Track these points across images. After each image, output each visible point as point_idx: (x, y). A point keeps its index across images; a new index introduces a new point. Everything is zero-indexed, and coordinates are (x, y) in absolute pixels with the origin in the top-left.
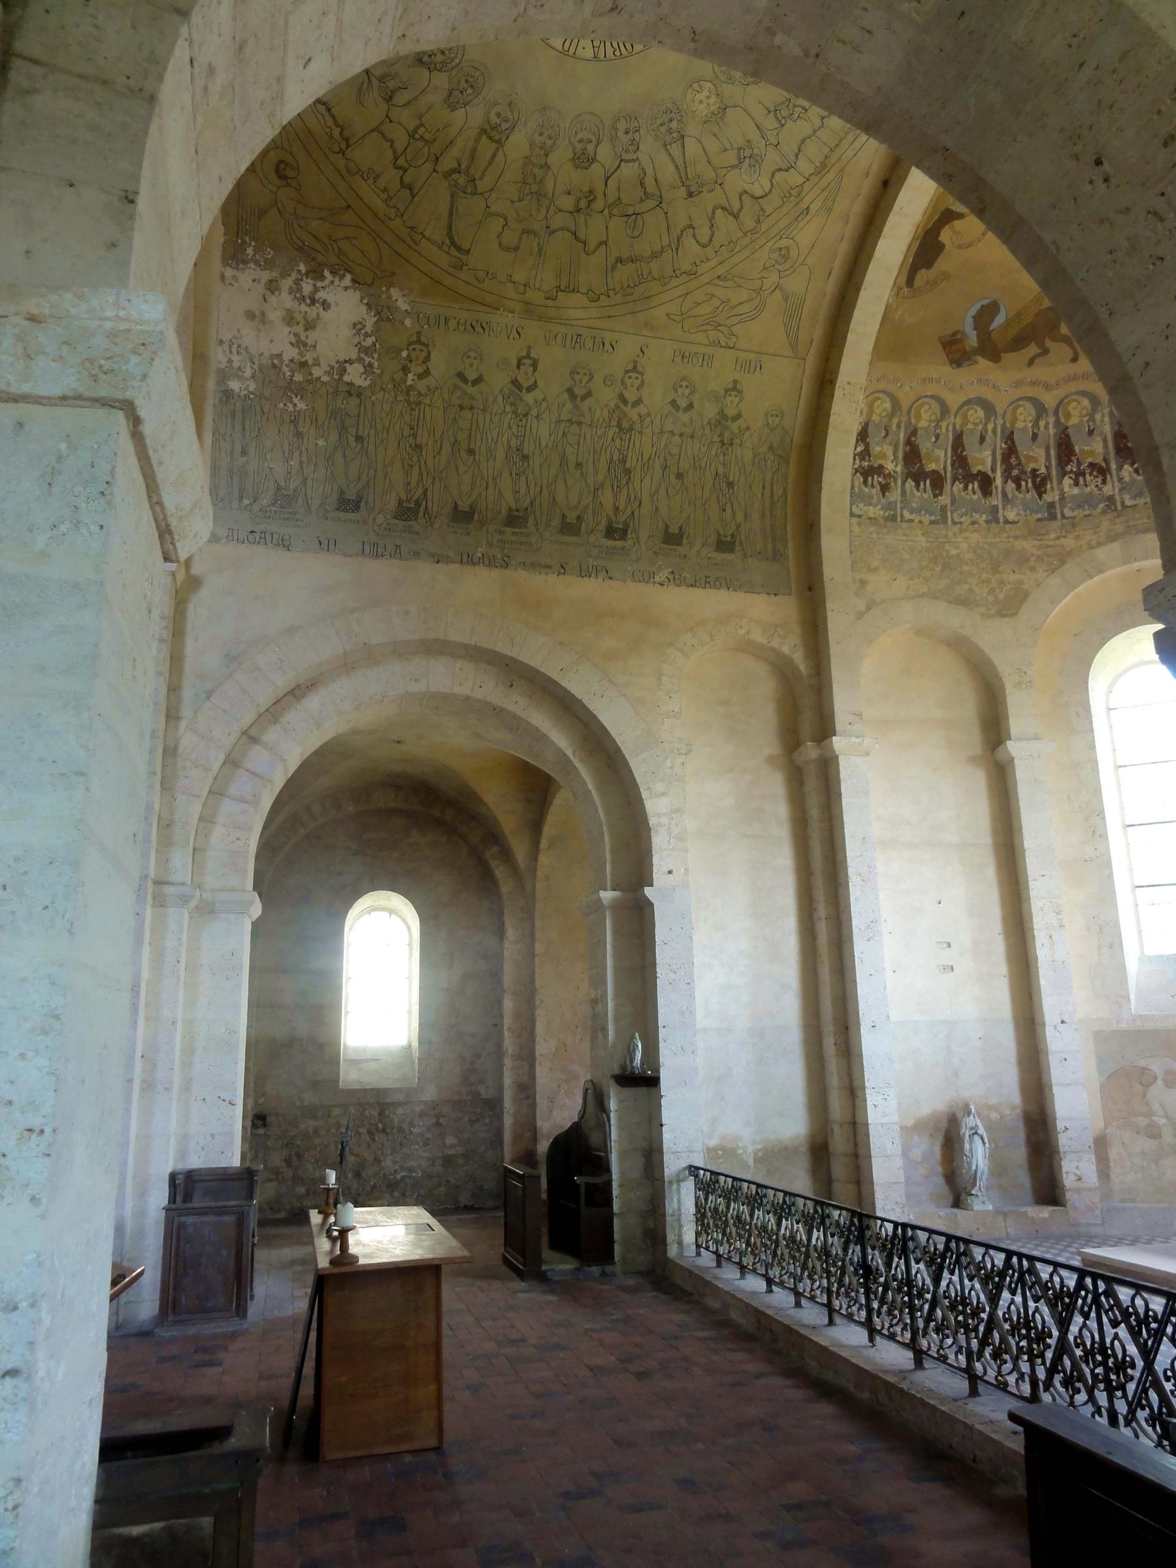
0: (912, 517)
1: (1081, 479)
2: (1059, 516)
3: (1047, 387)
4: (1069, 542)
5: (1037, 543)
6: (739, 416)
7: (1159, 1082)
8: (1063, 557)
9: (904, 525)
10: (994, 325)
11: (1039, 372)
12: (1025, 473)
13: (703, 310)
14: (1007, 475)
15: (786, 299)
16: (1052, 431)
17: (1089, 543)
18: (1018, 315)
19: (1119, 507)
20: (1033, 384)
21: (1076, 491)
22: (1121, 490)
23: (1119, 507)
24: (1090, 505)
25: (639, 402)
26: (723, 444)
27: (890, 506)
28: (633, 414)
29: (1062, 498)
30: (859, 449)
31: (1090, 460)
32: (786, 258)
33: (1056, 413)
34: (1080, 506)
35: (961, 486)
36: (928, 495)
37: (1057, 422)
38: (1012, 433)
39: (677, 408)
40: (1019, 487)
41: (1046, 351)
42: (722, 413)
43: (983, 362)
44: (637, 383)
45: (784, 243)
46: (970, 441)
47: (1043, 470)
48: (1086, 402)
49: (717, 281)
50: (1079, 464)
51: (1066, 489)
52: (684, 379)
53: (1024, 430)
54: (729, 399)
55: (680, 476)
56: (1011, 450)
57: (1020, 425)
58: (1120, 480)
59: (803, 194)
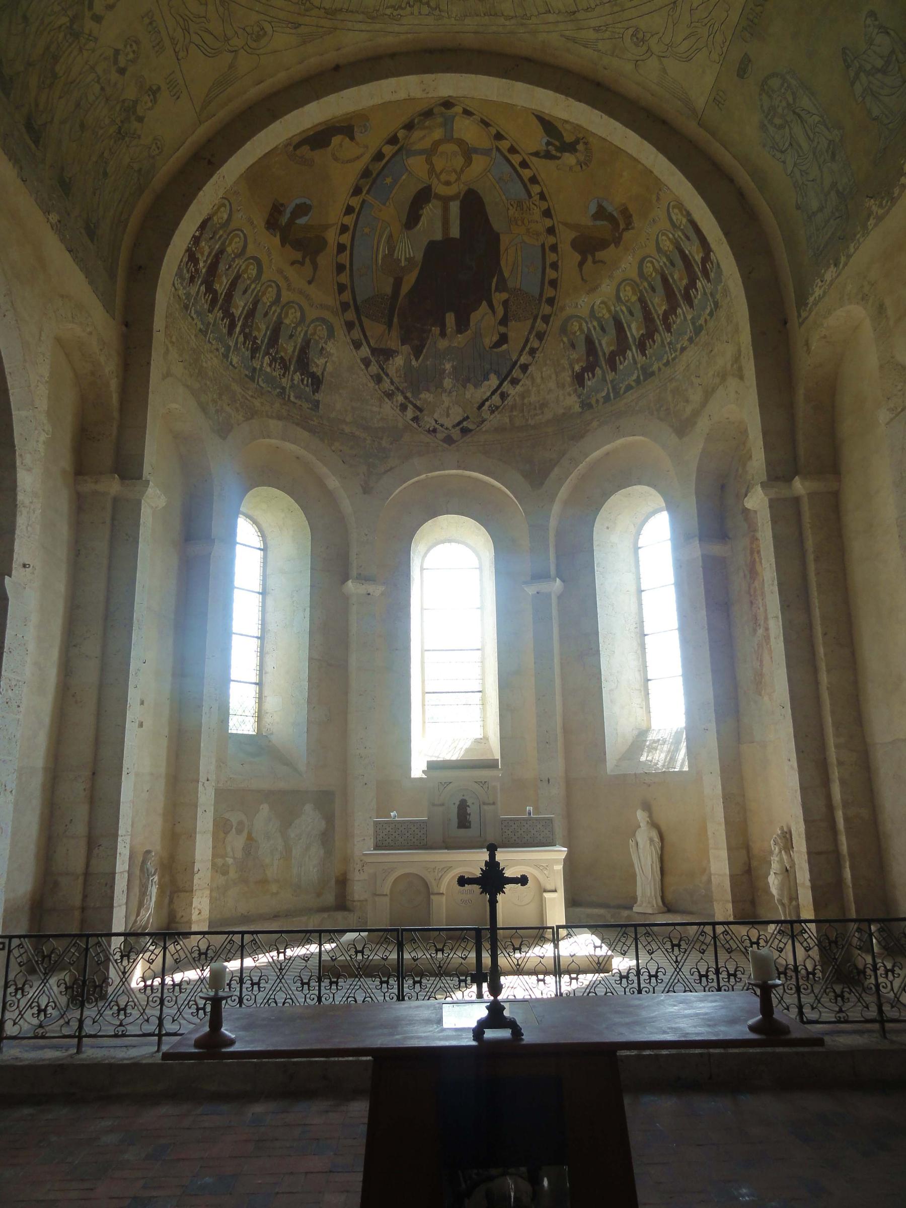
0: (195, 316)
3: (289, 288)
4: (257, 403)
7: (234, 829)
10: (298, 221)
12: (250, 334)
14: (242, 331)
20: (286, 279)
21: (268, 370)
22: (291, 387)
25: (98, 19)
26: (119, 132)
27: (188, 296)
28: (89, 25)
29: (261, 369)
30: (197, 234)
31: (282, 354)
36: (206, 307)
37: (280, 314)
38: (258, 301)
39: (116, 62)
41: (302, 264)
42: (136, 102)
43: (277, 240)
46: (241, 287)
48: (298, 314)
50: (277, 353)
51: (265, 365)
52: (137, 42)
53: (264, 304)
55: (82, 126)
56: (251, 314)
57: (264, 299)
58: (292, 380)
59: (308, 13)
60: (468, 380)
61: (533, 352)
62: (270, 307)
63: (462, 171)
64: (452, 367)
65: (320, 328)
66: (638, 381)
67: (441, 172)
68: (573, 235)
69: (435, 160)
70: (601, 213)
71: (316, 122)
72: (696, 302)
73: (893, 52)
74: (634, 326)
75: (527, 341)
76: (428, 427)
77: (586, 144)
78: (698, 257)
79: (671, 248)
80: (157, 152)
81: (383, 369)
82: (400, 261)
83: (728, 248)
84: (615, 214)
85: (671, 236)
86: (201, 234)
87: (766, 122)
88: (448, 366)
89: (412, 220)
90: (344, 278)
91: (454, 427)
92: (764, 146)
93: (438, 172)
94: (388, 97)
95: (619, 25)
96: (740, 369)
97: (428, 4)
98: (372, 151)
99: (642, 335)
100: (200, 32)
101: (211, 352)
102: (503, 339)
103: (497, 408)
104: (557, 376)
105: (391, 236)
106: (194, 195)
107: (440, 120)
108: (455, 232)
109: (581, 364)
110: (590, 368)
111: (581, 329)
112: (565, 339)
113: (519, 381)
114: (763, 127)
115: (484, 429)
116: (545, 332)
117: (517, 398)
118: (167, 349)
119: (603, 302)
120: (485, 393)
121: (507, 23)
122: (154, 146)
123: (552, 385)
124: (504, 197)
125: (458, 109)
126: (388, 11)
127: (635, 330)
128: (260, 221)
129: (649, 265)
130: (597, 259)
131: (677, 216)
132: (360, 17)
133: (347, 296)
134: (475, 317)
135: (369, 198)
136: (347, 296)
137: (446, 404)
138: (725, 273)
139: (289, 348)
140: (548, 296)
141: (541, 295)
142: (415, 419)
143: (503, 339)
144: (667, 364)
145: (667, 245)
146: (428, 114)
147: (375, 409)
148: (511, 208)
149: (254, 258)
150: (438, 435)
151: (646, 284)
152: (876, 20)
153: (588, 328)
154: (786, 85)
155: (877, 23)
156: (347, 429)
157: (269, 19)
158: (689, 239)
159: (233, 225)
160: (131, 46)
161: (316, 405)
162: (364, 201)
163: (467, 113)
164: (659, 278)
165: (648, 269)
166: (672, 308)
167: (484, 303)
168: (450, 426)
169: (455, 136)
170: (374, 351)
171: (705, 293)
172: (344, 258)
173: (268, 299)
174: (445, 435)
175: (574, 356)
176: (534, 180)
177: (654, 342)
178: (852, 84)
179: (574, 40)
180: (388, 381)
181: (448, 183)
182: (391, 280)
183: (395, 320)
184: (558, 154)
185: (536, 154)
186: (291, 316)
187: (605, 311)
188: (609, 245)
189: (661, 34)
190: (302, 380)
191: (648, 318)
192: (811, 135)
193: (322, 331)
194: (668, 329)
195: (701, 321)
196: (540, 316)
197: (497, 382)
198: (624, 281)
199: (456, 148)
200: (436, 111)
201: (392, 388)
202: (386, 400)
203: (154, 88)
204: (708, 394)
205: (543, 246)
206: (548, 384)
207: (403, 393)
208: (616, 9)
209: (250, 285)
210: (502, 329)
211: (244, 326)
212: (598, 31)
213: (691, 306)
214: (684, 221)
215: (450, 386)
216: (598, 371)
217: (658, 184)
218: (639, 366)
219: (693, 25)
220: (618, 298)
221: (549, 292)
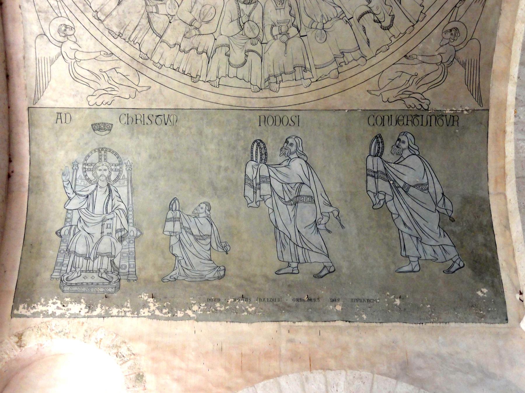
73: (210, 236)
87: (80, 166)
92: (63, 174)
95: (68, 12)
114: (75, 165)
152: (209, 211)
154: (118, 167)
155: (207, 212)
178: (167, 220)
192: (109, 210)
219: (104, 74)
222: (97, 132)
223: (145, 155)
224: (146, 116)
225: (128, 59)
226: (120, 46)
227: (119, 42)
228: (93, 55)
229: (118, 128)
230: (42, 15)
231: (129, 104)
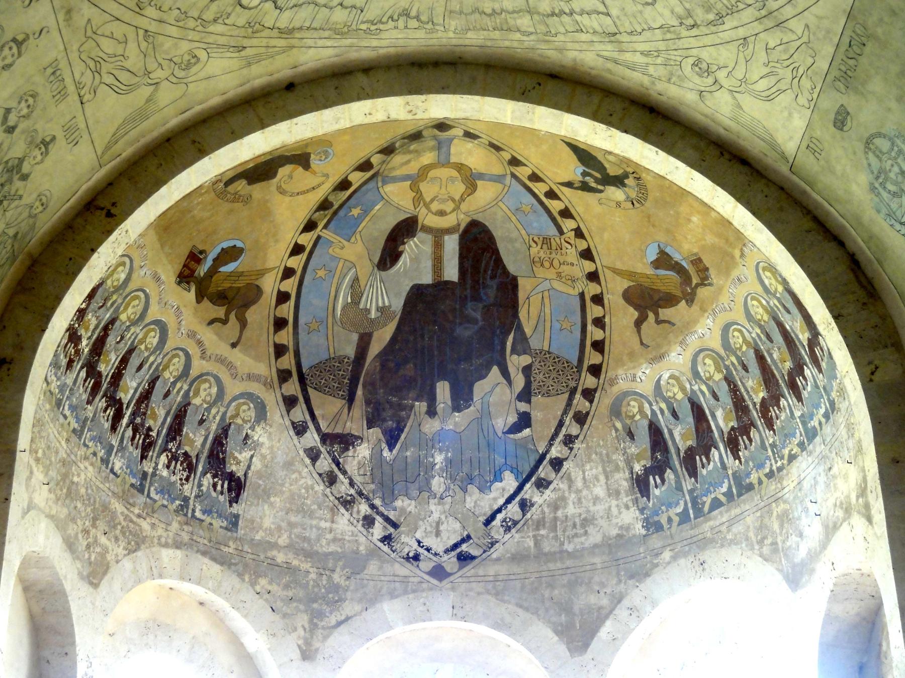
1: (174, 462)
2: (146, 493)
4: (145, 525)
5: (126, 512)
6: (25, 178)
8: (136, 542)
9: (61, 419)
10: (222, 269)
11: (208, 335)
12: (143, 425)
13: (108, 46)
14: (131, 422)
15: (148, 101)
16: (179, 399)
17: (159, 537)
18: (241, 274)
19: (190, 515)
20: (200, 343)
21: (165, 473)
22: (197, 497)
23: (190, 515)
24: (170, 496)
27: (62, 388)
29: (154, 474)
30: (84, 306)
31: (187, 448)
32: (189, 66)
33: (191, 385)
34: (161, 492)
35: (105, 405)
36: (85, 397)
38: (158, 377)
39: (5, 118)
40: (133, 438)
41: (225, 322)
42: (21, 161)
43: (192, 295)
44: (9, 61)
45: (202, 55)
46: (134, 362)
47: (154, 434)
48: (214, 390)
49: (141, 32)
50: (179, 447)
51: (160, 467)
53: (165, 381)
54: (37, 152)
56: (145, 397)
57: (167, 374)
58: (200, 485)
60: (470, 479)
61: (569, 441)
62: (174, 384)
63: (462, 199)
64: (446, 459)
65: (245, 407)
66: (729, 495)
67: (432, 201)
68: (626, 284)
69: (423, 186)
70: (663, 260)
71: (258, 153)
72: (805, 394)
74: (719, 414)
75: (561, 424)
76: (406, 550)
77: (638, 179)
78: (804, 337)
79: (766, 317)
80: (41, 208)
81: (338, 464)
82: (368, 311)
83: (840, 338)
84: (684, 264)
85: (764, 302)
86: (88, 305)
87: (877, 185)
88: (439, 458)
89: (390, 255)
90: (285, 337)
91: (447, 551)
93: (428, 200)
94: (359, 119)
95: (675, 53)
96: (867, 506)
97: (417, 18)
98: (334, 179)
99: (733, 428)
100: (114, 72)
101: (86, 458)
102: (524, 421)
103: (515, 523)
104: (607, 478)
105: (356, 279)
106: (86, 259)
107: (432, 143)
108: (451, 273)
109: (643, 462)
110: (659, 468)
111: (641, 411)
112: (619, 425)
113: (550, 483)
114: (873, 189)
115: (494, 556)
116: (588, 413)
117: (546, 510)
118: (31, 473)
119: (672, 377)
120: (495, 499)
121: (525, 38)
122: (38, 204)
123: (599, 491)
124: (523, 232)
125: (458, 132)
126: (364, 27)
127: (722, 420)
128: (169, 274)
129: (736, 334)
130: (662, 317)
131: (769, 280)
132: (327, 34)
133: (287, 361)
134: (480, 388)
135: (326, 234)
136: (287, 361)
137: (436, 516)
138: (838, 367)
139: (196, 440)
140: (592, 362)
141: (581, 360)
142: (387, 539)
143: (524, 421)
144: (770, 475)
145: (759, 313)
146: (416, 136)
147: (323, 524)
148: (534, 245)
149: (157, 322)
150: (422, 564)
151: (733, 359)
153: (653, 411)
154: (896, 149)
156: (280, 558)
157: (205, 46)
158: (788, 312)
159: (132, 286)
160: (27, 101)
161: (234, 522)
162: (319, 237)
163: (468, 135)
164: (751, 353)
165: (736, 340)
166: (774, 398)
167: (495, 369)
168: (440, 549)
169: (453, 159)
170: (325, 438)
171: (817, 387)
172: (286, 312)
173: (168, 376)
174: (431, 565)
175: (633, 450)
176: (566, 213)
177: (750, 440)
179: (616, 62)
180: (346, 481)
181: (442, 213)
182: (355, 337)
183: (360, 392)
184: (600, 187)
185: (569, 185)
186: (203, 394)
187: (676, 390)
188: (678, 302)
189: (730, 69)
190: (215, 486)
191: (740, 406)
193: (248, 412)
194: (770, 425)
195: (814, 423)
196: (580, 389)
197: (515, 484)
198: (701, 351)
199: (455, 173)
200: (425, 133)
201: (352, 491)
202: (342, 510)
203: (48, 139)
204: (831, 529)
205: (582, 295)
206: (595, 490)
207: (368, 499)
208: (668, 36)
209: (148, 357)
210: (523, 407)
211: (134, 414)
212: (646, 55)
213: (799, 398)
214: (780, 288)
215: (442, 490)
216: (669, 475)
217: (740, 238)
218: (730, 472)
219: (771, 64)
220: (696, 374)
221: (593, 358)
222: (845, 128)
223: (893, 105)
224: (845, 59)
225: (757, 27)
226: (735, 24)
227: (730, 23)
228: (742, 61)
229: (851, 101)
230: (674, 79)
231: (823, 64)
